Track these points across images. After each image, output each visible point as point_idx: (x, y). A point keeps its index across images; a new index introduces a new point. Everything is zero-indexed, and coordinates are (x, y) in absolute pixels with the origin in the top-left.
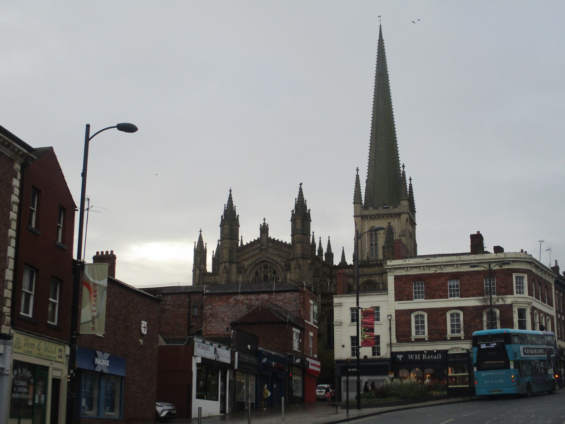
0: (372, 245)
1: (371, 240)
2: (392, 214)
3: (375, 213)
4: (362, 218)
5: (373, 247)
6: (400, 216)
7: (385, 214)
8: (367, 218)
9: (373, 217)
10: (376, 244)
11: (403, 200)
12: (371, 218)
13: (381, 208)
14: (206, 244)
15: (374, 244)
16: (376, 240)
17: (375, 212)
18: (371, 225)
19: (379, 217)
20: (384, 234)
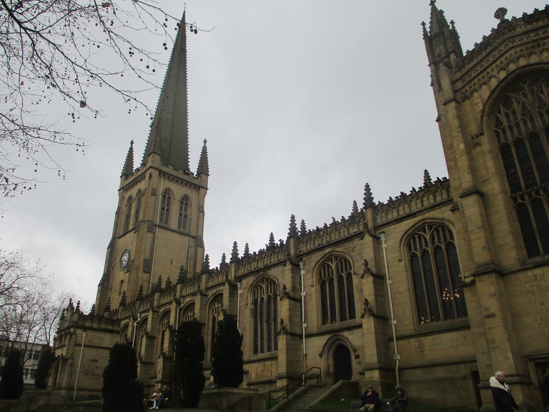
1: (163, 203)
2: (192, 183)
3: (175, 175)
4: (160, 174)
5: (164, 211)
6: (199, 189)
7: (184, 180)
8: (164, 176)
9: (171, 178)
10: (168, 210)
11: (204, 173)
12: (168, 177)
13: (181, 172)
15: (166, 209)
17: (175, 173)
19: (177, 181)
20: (179, 201)
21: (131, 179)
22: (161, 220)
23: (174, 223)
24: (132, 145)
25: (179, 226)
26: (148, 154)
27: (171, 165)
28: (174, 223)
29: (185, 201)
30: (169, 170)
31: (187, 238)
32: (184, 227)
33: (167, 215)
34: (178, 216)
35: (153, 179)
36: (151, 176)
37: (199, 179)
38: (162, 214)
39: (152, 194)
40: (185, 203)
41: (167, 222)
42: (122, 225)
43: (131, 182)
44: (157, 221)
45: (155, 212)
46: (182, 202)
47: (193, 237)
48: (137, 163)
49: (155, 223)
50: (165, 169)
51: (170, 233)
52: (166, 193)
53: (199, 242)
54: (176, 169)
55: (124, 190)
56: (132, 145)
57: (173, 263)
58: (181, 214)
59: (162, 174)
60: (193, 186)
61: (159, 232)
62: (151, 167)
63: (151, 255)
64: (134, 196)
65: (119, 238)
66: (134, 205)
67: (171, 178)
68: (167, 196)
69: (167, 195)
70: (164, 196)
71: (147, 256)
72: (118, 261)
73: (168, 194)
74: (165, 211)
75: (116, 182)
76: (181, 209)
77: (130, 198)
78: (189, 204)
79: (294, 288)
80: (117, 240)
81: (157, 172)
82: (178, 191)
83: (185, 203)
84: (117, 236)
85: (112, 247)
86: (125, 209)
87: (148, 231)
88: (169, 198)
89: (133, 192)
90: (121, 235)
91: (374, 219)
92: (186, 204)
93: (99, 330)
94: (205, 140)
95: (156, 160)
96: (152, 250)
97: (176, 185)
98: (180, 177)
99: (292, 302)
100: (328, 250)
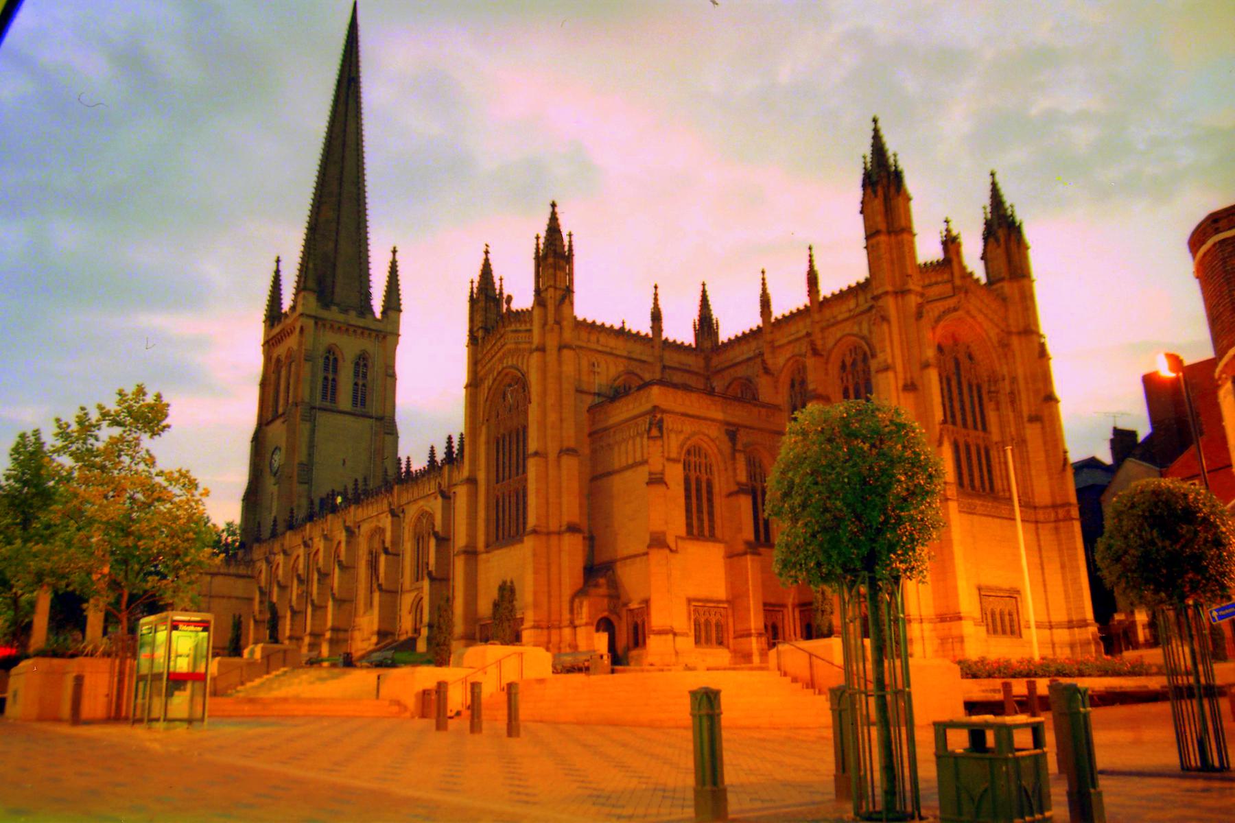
0: (326, 378)
1: (326, 369)
4: (316, 323)
6: (384, 337)
10: (334, 380)
13: (353, 314)
14: (570, 235)
16: (335, 371)
18: (332, 341)
21: (277, 330)
22: (324, 397)
23: (345, 400)
24: (278, 265)
25: (355, 404)
26: (301, 288)
27: (338, 305)
28: (345, 400)
29: (362, 362)
30: (334, 314)
31: (368, 422)
32: (363, 404)
33: (334, 388)
34: (350, 387)
35: (306, 332)
36: (302, 329)
37: (385, 320)
38: (325, 387)
39: (306, 360)
40: (362, 363)
41: (334, 400)
42: (271, 404)
43: (277, 334)
44: (318, 403)
45: (312, 390)
46: (357, 364)
47: (376, 419)
48: (287, 302)
49: (313, 405)
50: (325, 314)
51: (339, 417)
52: (329, 352)
53: (387, 426)
54: (345, 311)
55: (269, 346)
56: (278, 265)
57: (348, 463)
58: (356, 384)
59: (320, 323)
60: (374, 334)
61: (323, 419)
62: (302, 315)
63: (310, 455)
64: (283, 358)
65: (268, 423)
66: (284, 373)
67: (337, 326)
68: (331, 358)
69: (331, 360)
70: (327, 358)
71: (304, 459)
72: (267, 463)
73: (334, 353)
74: (330, 382)
75: (257, 332)
76: (356, 374)
77: (278, 360)
78: (370, 364)
79: (393, 543)
80: (264, 428)
81: (311, 322)
82: (350, 347)
83: (362, 363)
84: (265, 422)
85: (258, 440)
86: (273, 377)
87: (303, 420)
88: (336, 360)
89: (281, 350)
90: (270, 419)
91: (450, 476)
92: (365, 365)
93: (229, 575)
94: (395, 248)
95: (311, 303)
96: (311, 446)
97: (345, 336)
98: (352, 322)
99: (390, 557)
100: (421, 503)
